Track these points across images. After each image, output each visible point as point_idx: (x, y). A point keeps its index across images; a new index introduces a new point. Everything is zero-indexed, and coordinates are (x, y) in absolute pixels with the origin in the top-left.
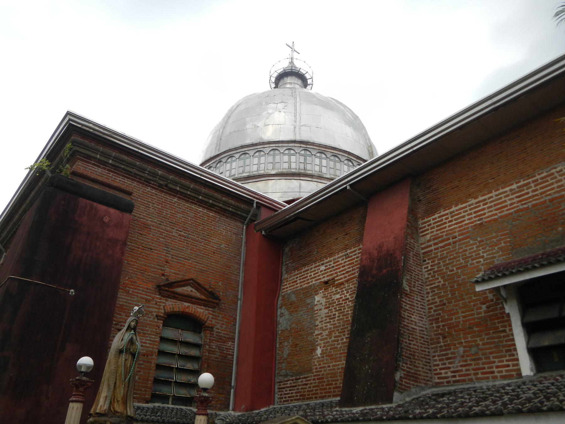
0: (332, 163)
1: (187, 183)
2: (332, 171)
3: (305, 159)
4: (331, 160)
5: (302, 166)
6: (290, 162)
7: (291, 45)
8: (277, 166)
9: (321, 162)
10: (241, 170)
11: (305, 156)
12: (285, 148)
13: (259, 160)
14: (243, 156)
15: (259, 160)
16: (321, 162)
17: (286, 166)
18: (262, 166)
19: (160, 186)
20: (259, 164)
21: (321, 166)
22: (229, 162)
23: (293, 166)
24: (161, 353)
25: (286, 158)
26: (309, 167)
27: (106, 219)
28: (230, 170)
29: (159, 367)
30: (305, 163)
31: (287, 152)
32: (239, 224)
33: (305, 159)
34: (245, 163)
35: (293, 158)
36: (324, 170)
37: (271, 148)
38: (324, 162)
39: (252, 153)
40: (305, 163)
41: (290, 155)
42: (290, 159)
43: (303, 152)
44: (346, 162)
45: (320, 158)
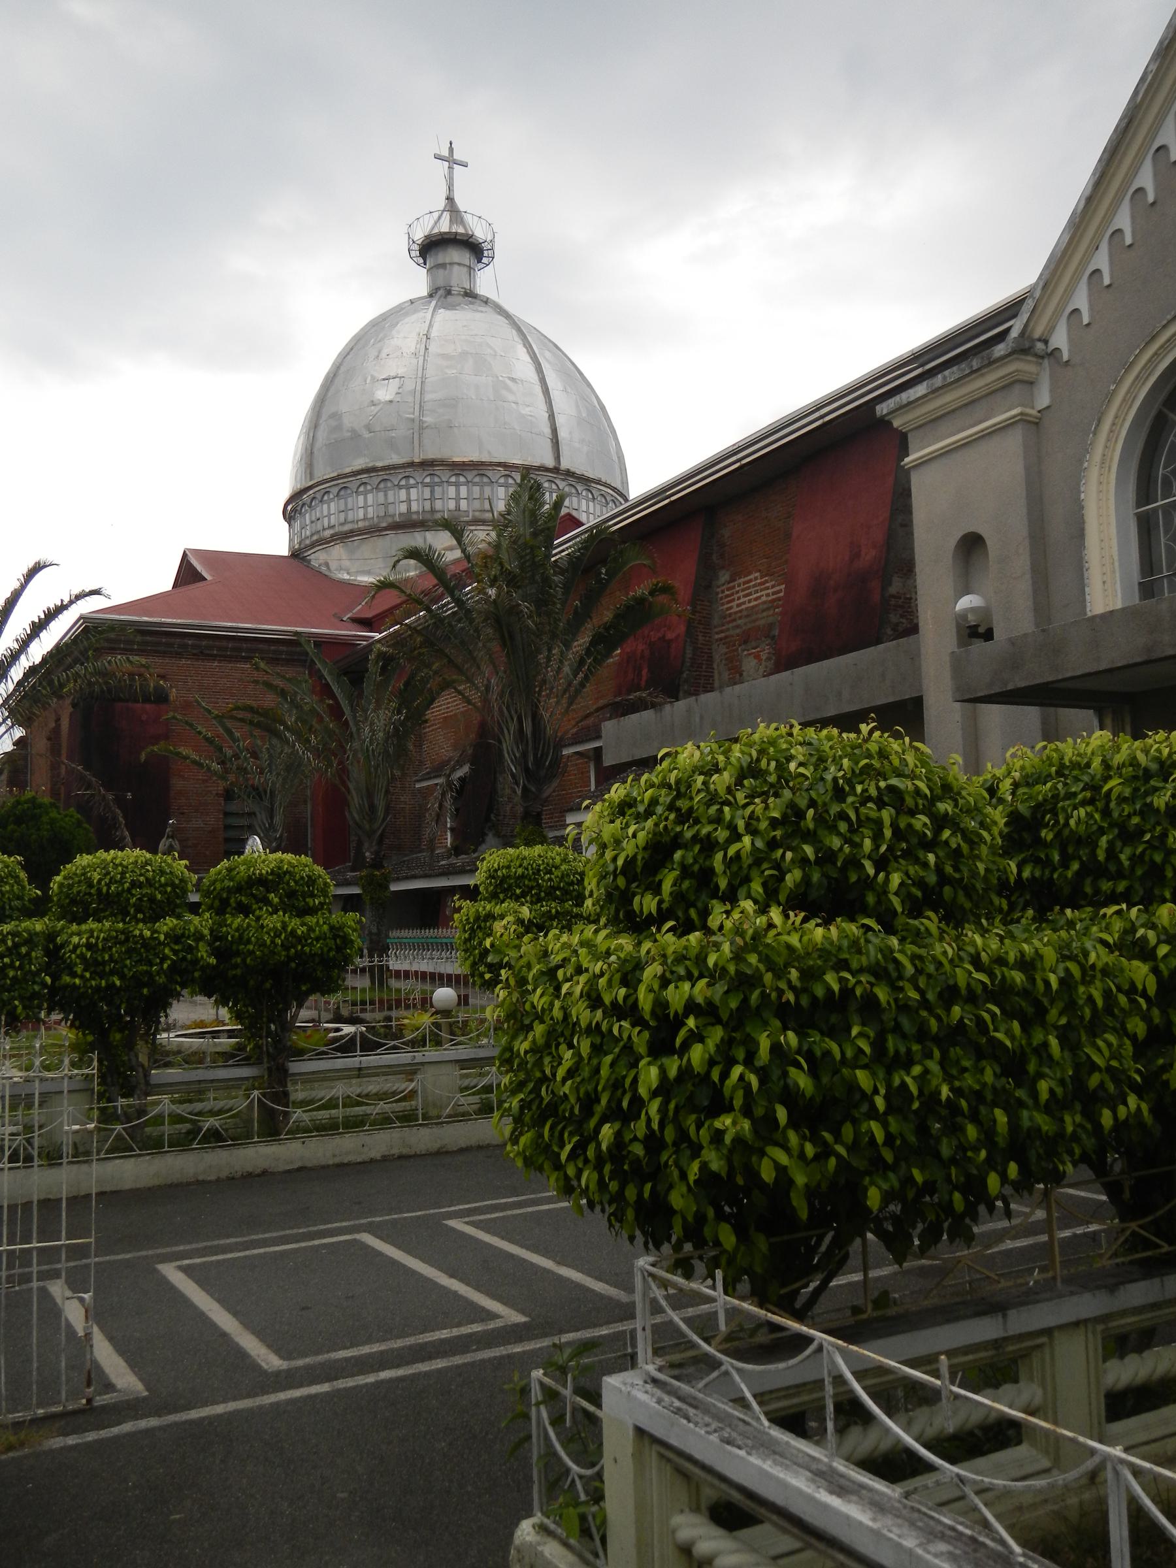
0: (476, 489)
1: (224, 643)
2: (477, 505)
3: (432, 492)
4: (475, 484)
5: (428, 506)
6: (409, 501)
7: (446, 153)
8: (391, 508)
9: (458, 492)
10: (342, 520)
11: (431, 486)
12: (400, 476)
13: (365, 500)
14: (342, 493)
15: (365, 500)
16: (458, 492)
17: (403, 508)
18: (370, 510)
19: (194, 655)
20: (365, 507)
21: (458, 499)
22: (326, 502)
23: (414, 507)
24: (227, 827)
25: (403, 494)
26: (438, 505)
27: (144, 717)
28: (329, 515)
29: (227, 840)
30: (432, 499)
31: (403, 483)
32: (302, 669)
33: (432, 492)
34: (346, 504)
35: (413, 492)
36: (464, 505)
37: (380, 478)
38: (463, 491)
39: (353, 486)
40: (432, 499)
41: (408, 488)
42: (408, 494)
43: (428, 480)
44: (502, 480)
45: (457, 485)
